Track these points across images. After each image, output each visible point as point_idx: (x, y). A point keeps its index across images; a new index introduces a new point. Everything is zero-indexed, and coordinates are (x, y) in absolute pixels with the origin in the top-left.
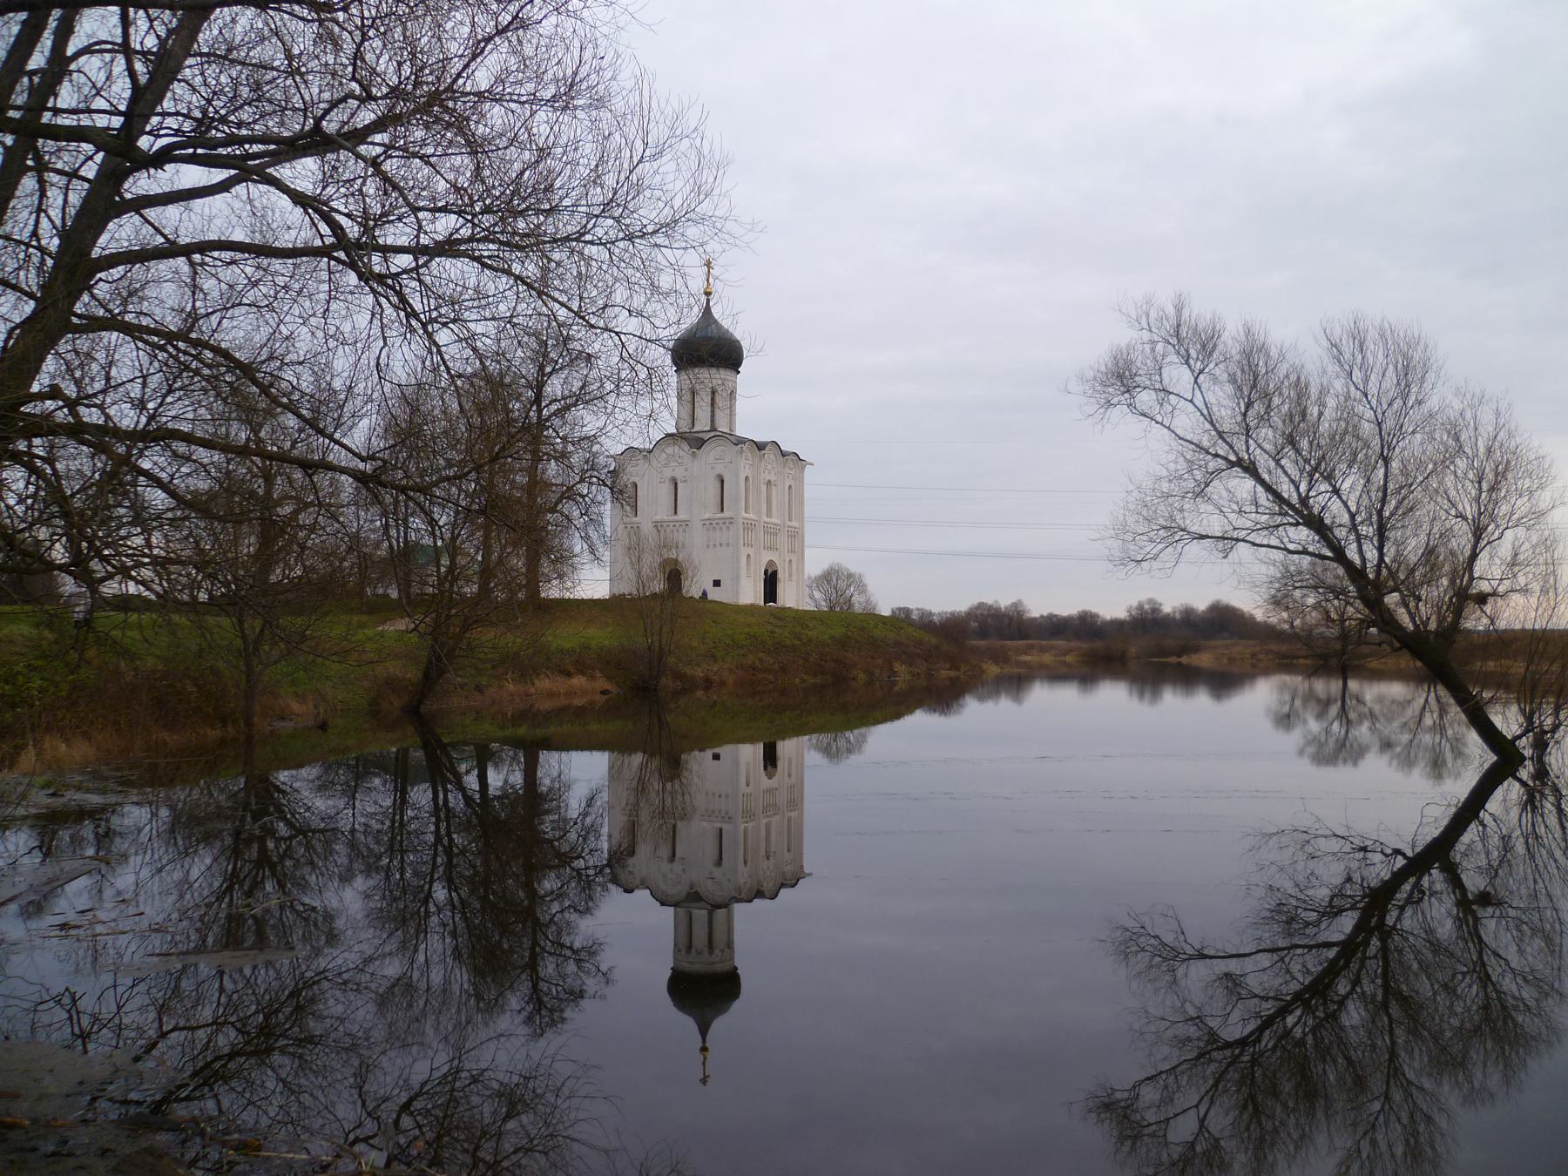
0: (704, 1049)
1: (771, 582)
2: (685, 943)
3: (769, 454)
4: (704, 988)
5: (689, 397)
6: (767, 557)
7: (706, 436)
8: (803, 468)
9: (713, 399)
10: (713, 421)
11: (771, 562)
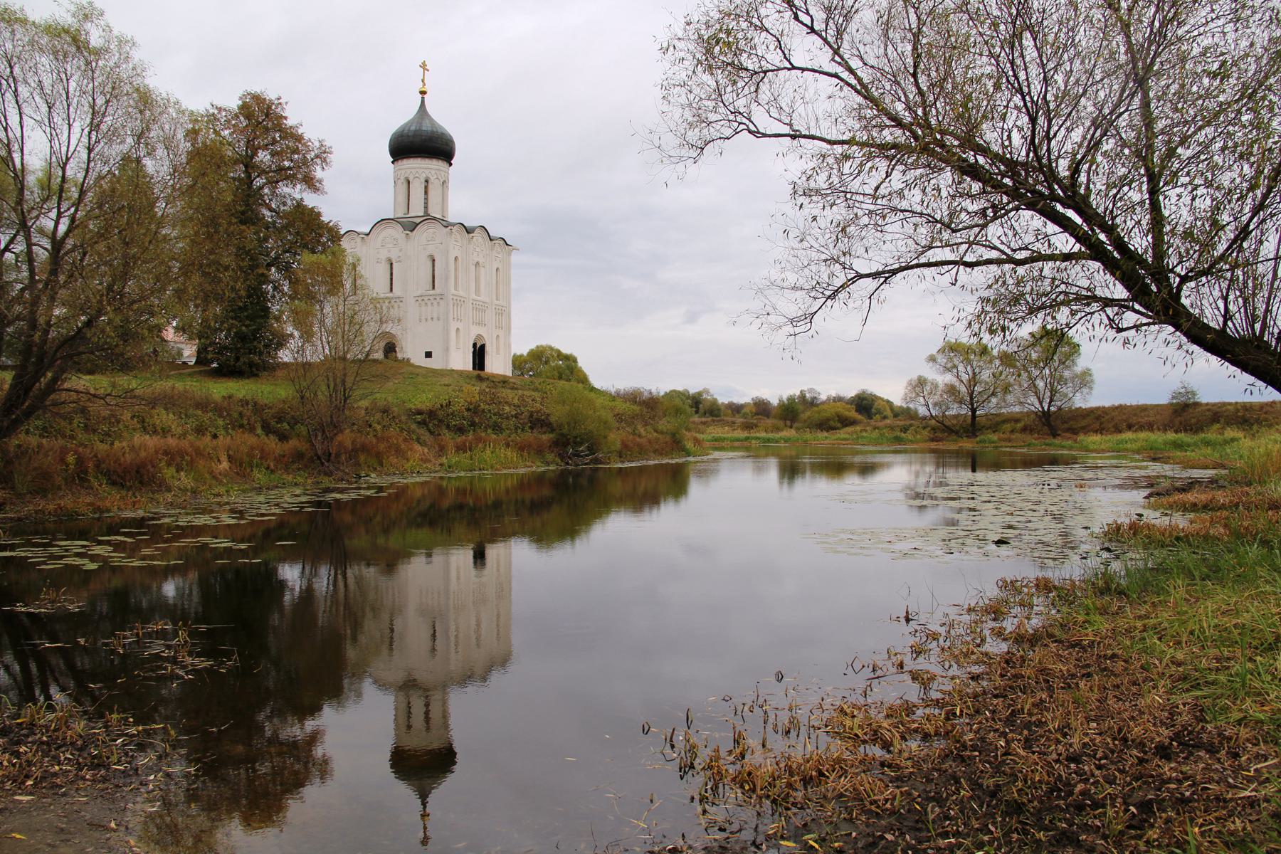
1: (479, 354)
2: (405, 721)
3: (478, 235)
4: (424, 764)
6: (475, 331)
7: (418, 220)
8: (509, 254)
9: (426, 187)
10: (426, 207)
11: (479, 336)
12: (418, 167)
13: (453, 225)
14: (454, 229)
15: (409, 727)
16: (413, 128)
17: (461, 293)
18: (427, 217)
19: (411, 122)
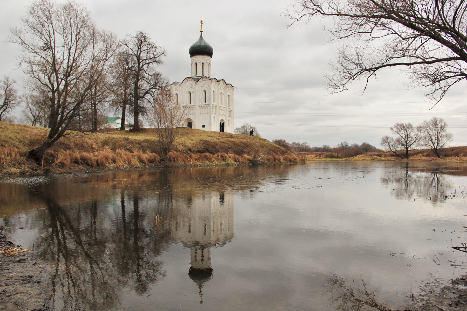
1: (222, 126)
3: (222, 84)
4: (200, 274)
6: (221, 118)
7: (200, 78)
8: (233, 89)
9: (203, 66)
10: (203, 73)
11: (222, 120)
13: (213, 79)
14: (213, 80)
15: (196, 260)
16: (198, 44)
17: (215, 104)
18: (203, 76)
19: (197, 42)
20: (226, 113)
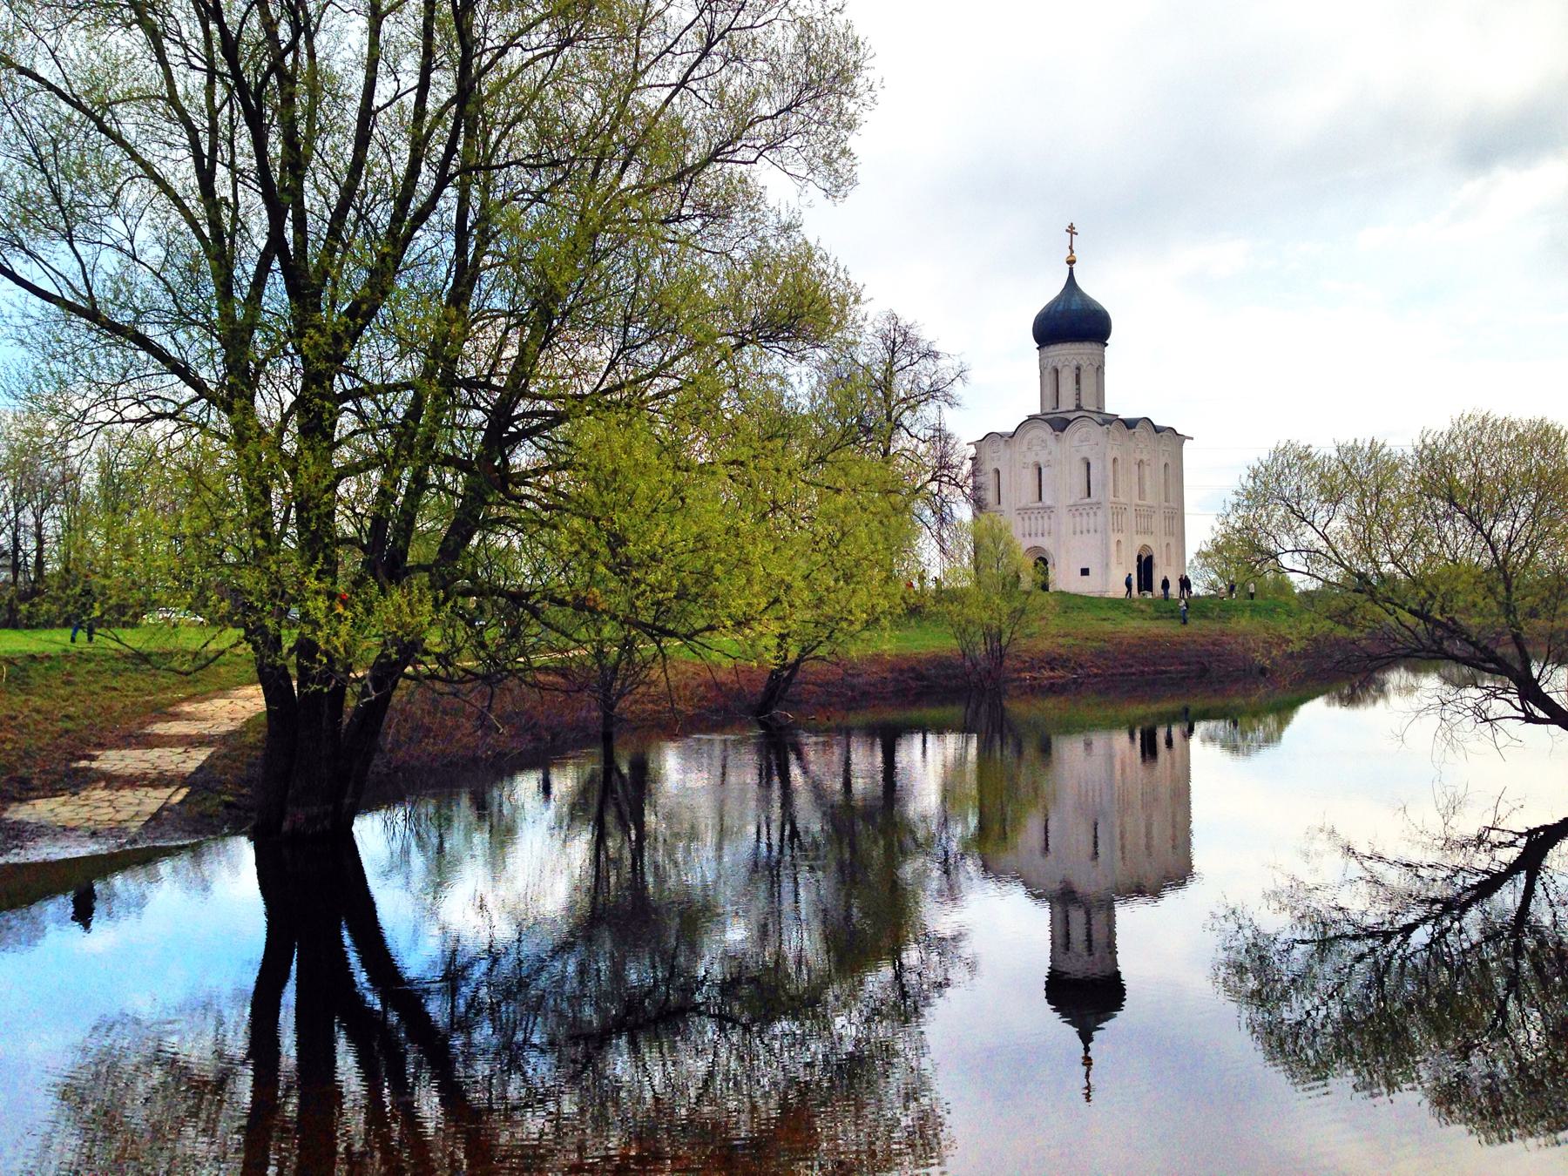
0: (1087, 1061)
5: (1051, 377)
7: (1071, 416)
11: (1145, 547)
12: (1068, 353)
17: (1122, 499)
20: (1158, 522)
